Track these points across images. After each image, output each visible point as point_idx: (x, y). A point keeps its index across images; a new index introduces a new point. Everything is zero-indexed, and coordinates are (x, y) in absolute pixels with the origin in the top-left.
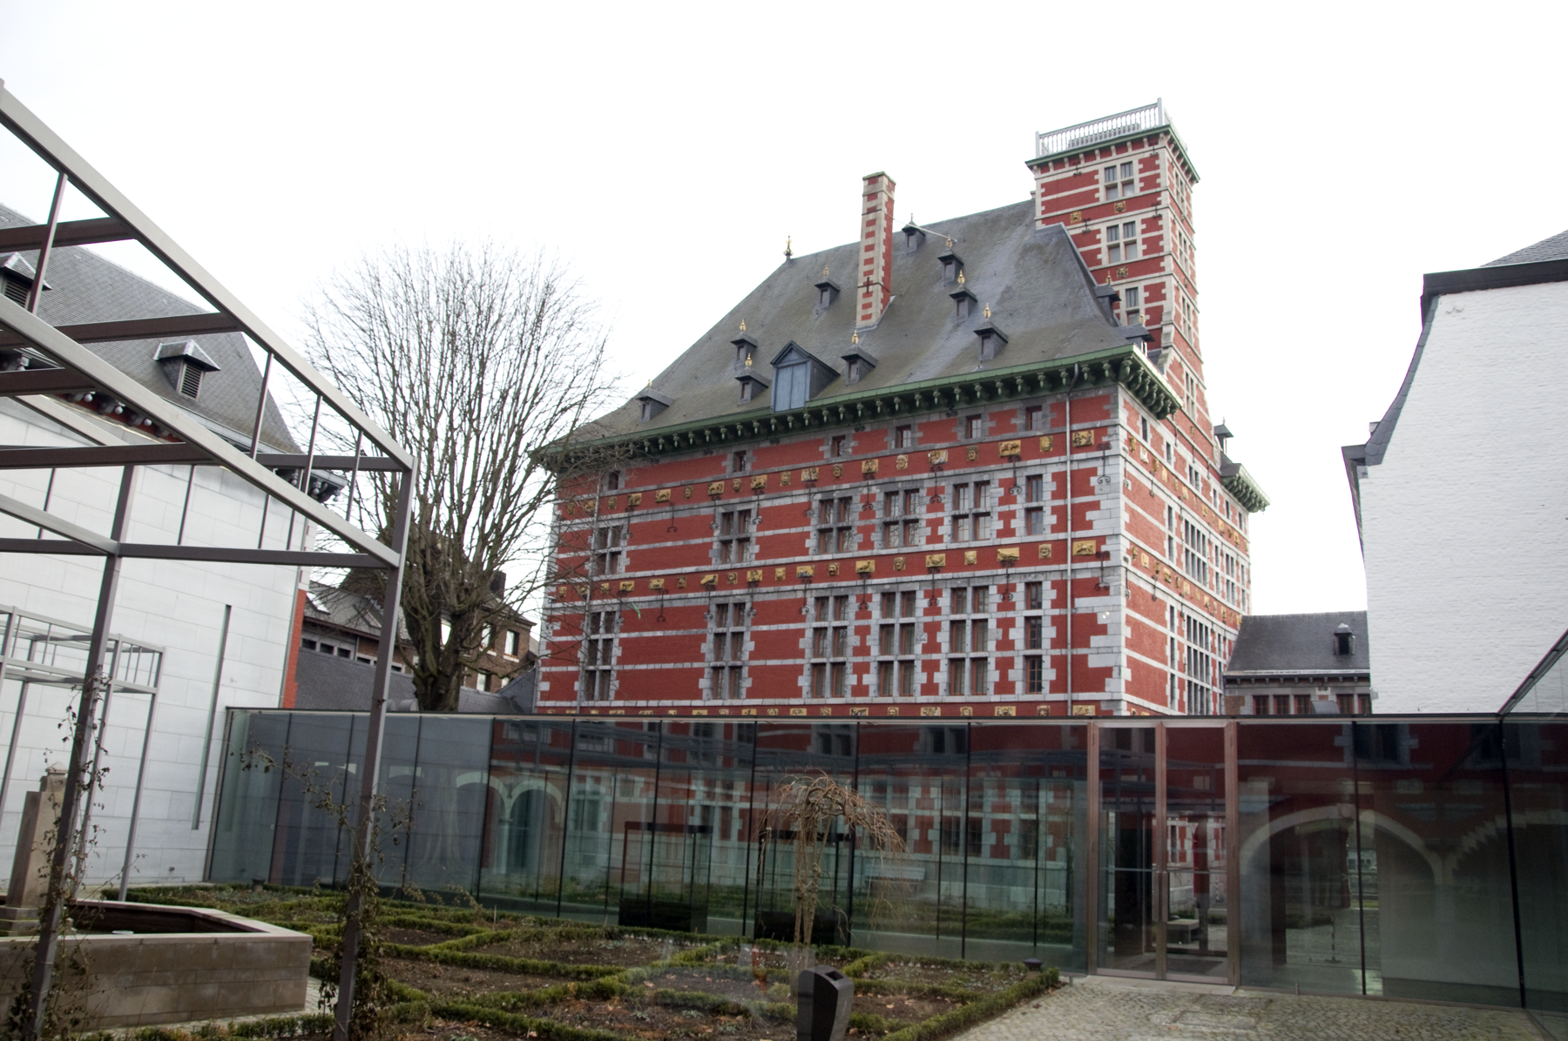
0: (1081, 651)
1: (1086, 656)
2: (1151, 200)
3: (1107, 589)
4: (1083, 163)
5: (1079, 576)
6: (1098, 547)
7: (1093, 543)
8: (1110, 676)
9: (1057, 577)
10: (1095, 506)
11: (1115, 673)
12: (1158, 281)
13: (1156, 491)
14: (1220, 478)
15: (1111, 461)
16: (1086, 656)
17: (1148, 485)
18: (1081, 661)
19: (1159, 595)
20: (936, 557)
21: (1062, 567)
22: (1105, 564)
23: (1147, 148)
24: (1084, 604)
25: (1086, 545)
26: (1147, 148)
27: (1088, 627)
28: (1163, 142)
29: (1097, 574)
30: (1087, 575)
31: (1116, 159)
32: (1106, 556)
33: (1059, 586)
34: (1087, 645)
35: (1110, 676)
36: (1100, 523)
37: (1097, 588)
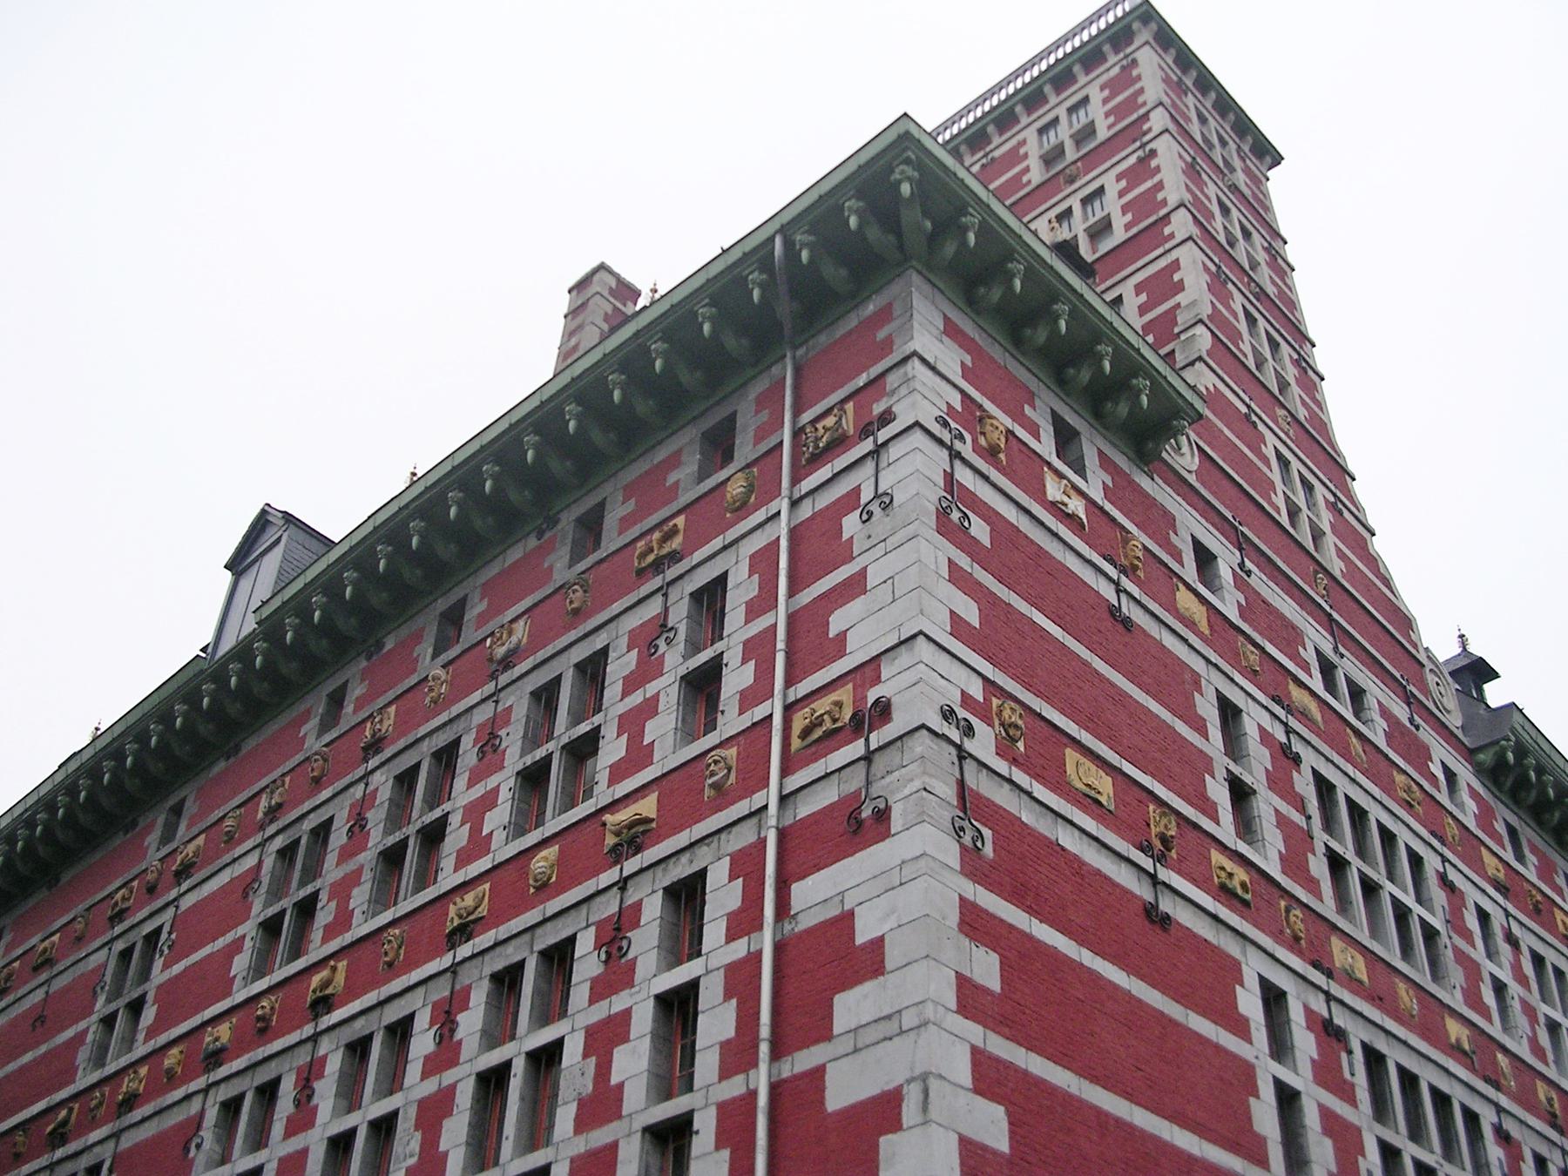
0: (803, 1060)
1: (818, 1073)
2: (1133, 132)
3: (882, 815)
4: (996, 140)
5: (805, 808)
6: (859, 698)
7: (845, 694)
8: (895, 1125)
9: (742, 838)
10: (855, 586)
11: (910, 1111)
12: (1162, 263)
13: (1128, 608)
14: (1469, 754)
15: (895, 451)
16: (818, 1073)
17: (1108, 592)
18: (796, 1098)
19: (1167, 905)
20: (469, 899)
21: (757, 800)
22: (876, 739)
23: (1112, 59)
24: (815, 895)
25: (822, 705)
26: (1112, 59)
27: (834, 958)
28: (1144, 35)
29: (854, 781)
30: (828, 795)
31: (1057, 106)
32: (883, 710)
33: (746, 865)
34: (822, 1031)
35: (895, 1125)
36: (861, 629)
37: (860, 825)
